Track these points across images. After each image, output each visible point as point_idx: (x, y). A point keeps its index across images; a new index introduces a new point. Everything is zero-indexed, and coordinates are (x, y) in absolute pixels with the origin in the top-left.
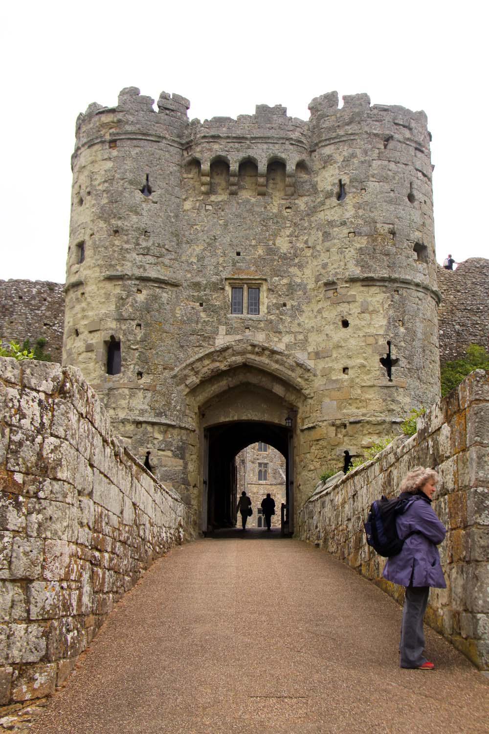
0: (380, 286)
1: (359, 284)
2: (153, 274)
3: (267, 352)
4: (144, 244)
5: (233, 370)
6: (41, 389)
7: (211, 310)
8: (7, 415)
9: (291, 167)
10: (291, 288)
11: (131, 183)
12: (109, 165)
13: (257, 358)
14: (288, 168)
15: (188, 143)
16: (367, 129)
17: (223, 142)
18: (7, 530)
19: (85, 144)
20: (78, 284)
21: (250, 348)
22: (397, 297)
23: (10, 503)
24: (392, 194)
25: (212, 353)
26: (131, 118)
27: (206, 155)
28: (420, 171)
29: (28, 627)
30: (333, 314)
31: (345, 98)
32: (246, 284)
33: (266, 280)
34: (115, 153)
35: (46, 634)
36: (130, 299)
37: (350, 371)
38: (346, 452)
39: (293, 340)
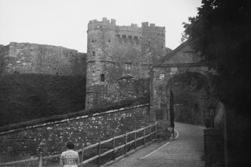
27: (121, 34)
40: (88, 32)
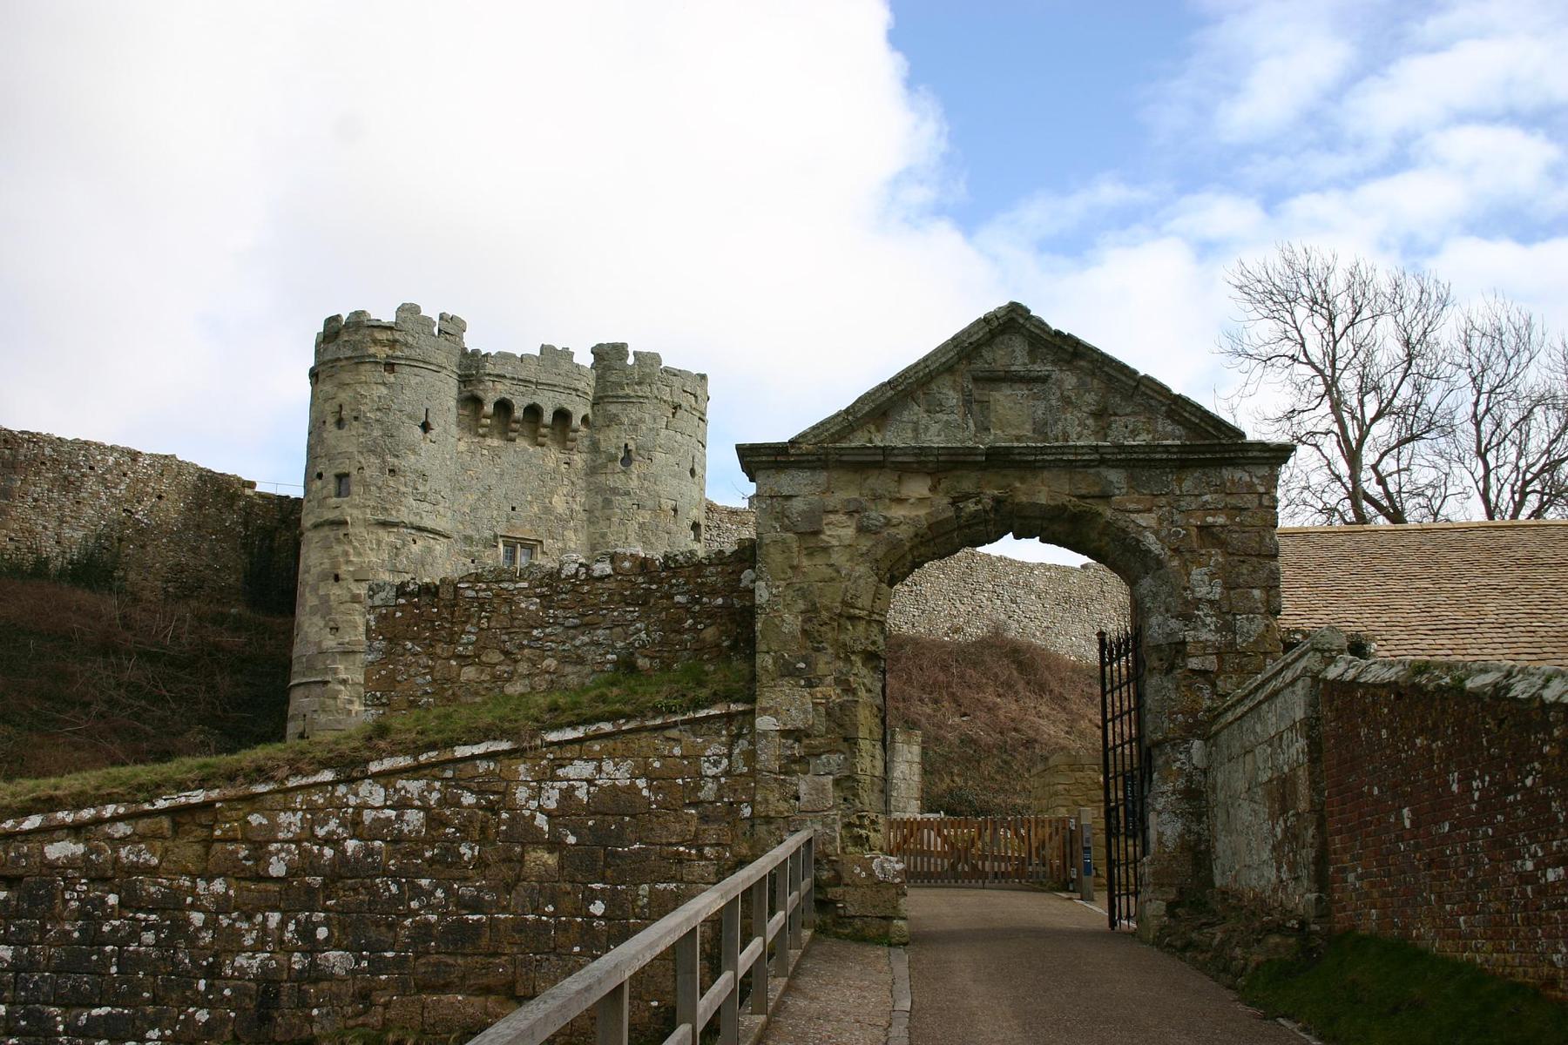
2: (428, 522)
4: (421, 489)
9: (576, 421)
12: (384, 391)
17: (507, 382)
26: (410, 339)
27: (491, 395)
34: (391, 378)
40: (314, 375)
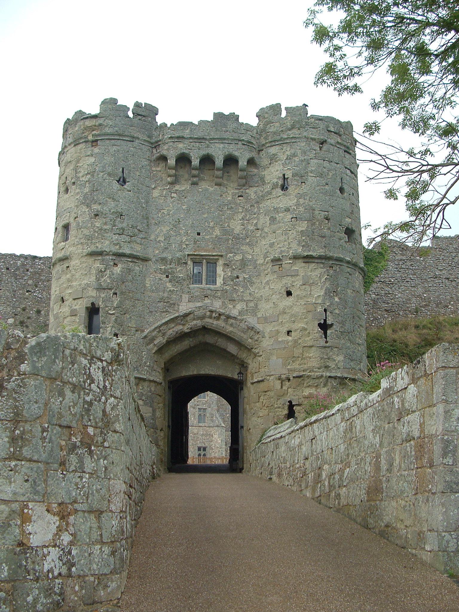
0: (318, 263)
1: (300, 261)
3: (223, 317)
4: (120, 226)
5: (193, 333)
6: (104, 359)
7: (175, 280)
8: (82, 380)
9: (242, 163)
10: (244, 263)
11: (109, 175)
12: (92, 160)
13: (215, 322)
14: (240, 163)
15: (157, 142)
16: (305, 134)
17: (187, 142)
18: (84, 472)
19: (72, 143)
20: (65, 259)
21: (208, 313)
22: (331, 272)
23: (86, 451)
24: (327, 187)
25: (176, 318)
28: (349, 169)
29: (102, 547)
30: (279, 286)
31: (286, 109)
32: (206, 259)
33: (222, 256)
34: (96, 150)
35: (113, 553)
36: (108, 272)
37: (293, 334)
38: (290, 402)
39: (245, 307)
